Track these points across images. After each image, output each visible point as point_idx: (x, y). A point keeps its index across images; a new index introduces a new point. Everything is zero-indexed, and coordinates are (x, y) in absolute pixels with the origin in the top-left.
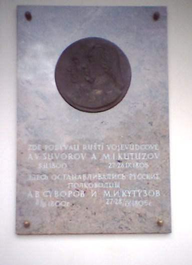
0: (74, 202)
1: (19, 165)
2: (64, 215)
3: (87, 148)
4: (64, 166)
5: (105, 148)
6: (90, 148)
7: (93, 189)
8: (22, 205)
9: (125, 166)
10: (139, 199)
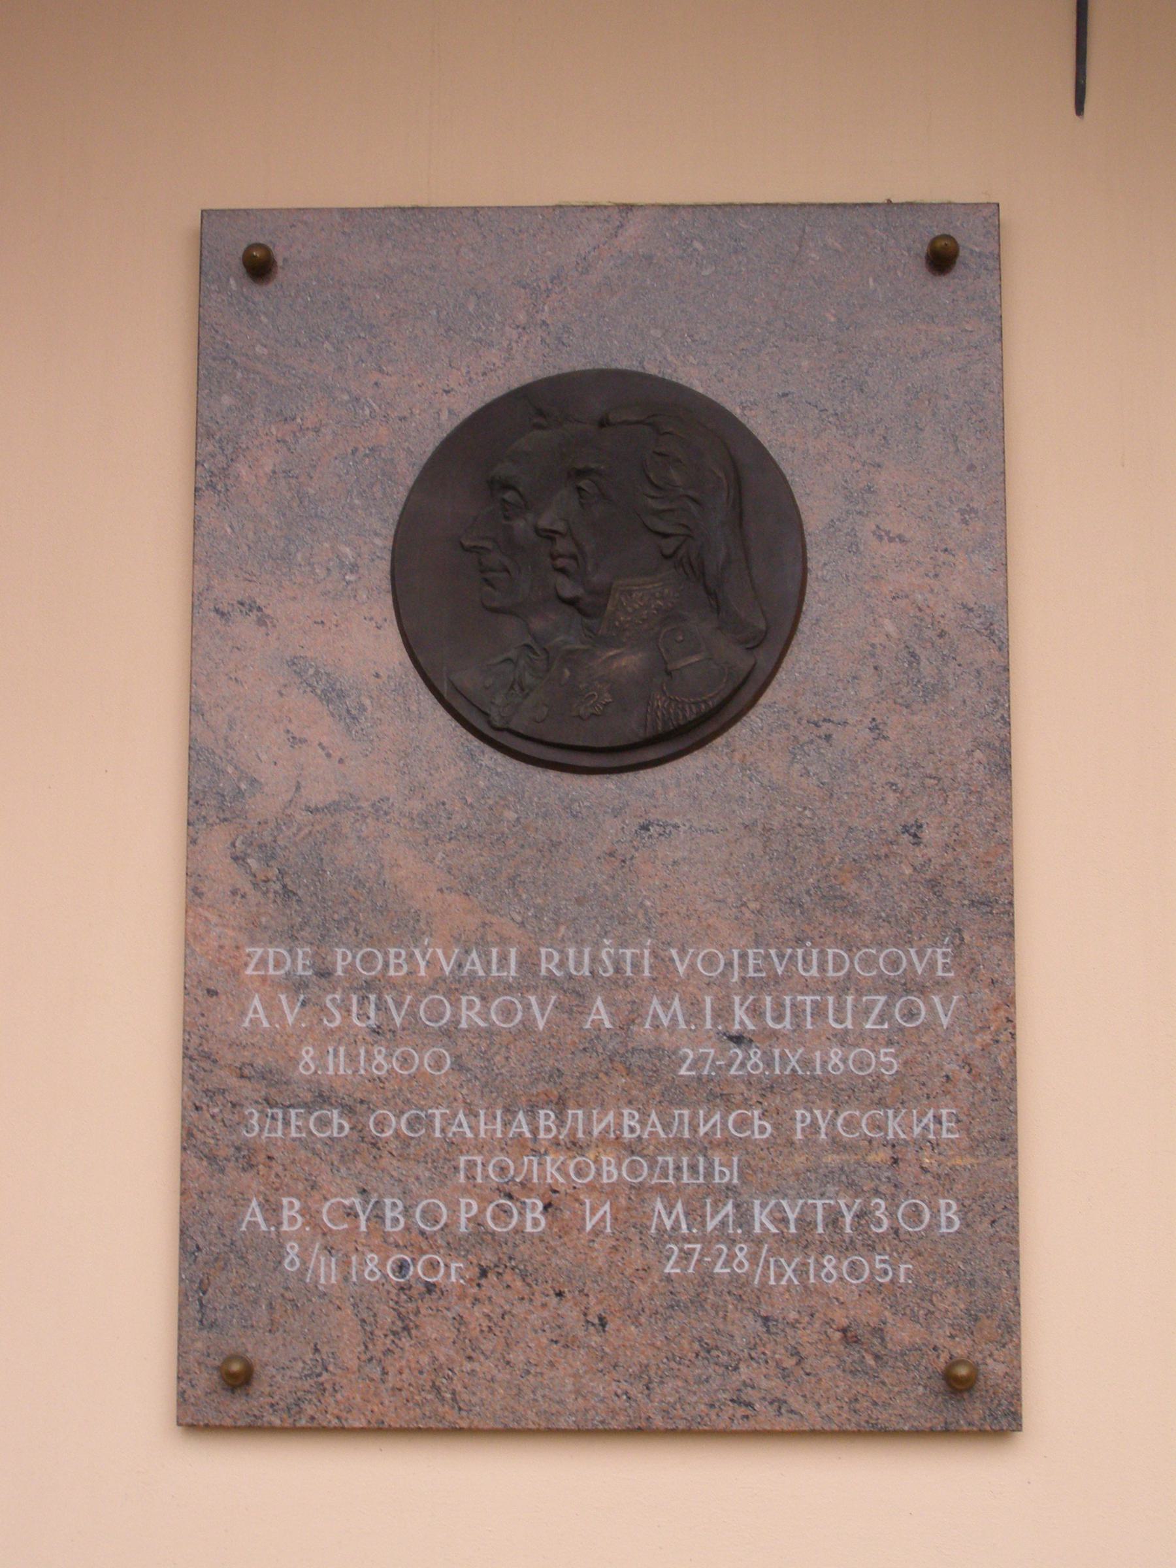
0: (488, 1258)
1: (198, 1058)
2: (433, 1328)
3: (562, 964)
4: (438, 1063)
5: (661, 961)
6: (579, 964)
7: (591, 1187)
8: (212, 1269)
9: (769, 1064)
10: (846, 1248)
